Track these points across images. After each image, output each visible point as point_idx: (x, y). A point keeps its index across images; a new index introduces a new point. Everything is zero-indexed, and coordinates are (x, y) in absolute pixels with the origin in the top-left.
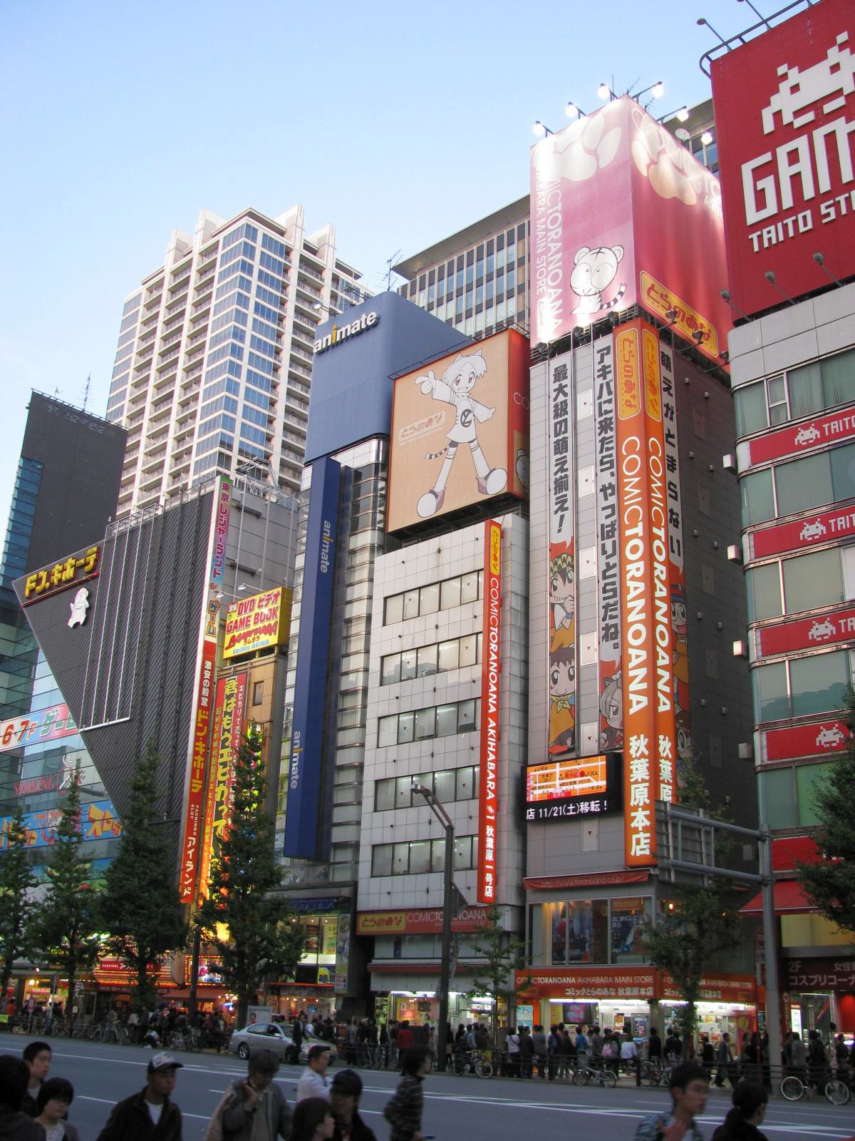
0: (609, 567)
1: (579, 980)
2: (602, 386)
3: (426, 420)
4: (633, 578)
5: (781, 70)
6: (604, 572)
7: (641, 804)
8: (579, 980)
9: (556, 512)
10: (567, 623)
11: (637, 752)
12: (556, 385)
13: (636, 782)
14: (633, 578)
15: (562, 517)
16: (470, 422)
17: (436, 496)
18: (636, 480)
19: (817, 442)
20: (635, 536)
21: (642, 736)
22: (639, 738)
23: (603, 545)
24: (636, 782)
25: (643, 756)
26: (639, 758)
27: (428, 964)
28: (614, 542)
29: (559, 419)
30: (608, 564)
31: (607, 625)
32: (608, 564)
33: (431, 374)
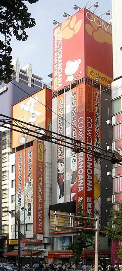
3: (22, 117)
11: (89, 201)
13: (88, 208)
16: (34, 116)
17: (25, 138)
21: (90, 198)
22: (89, 198)
24: (88, 208)
25: (90, 202)
26: (89, 203)
33: (23, 103)
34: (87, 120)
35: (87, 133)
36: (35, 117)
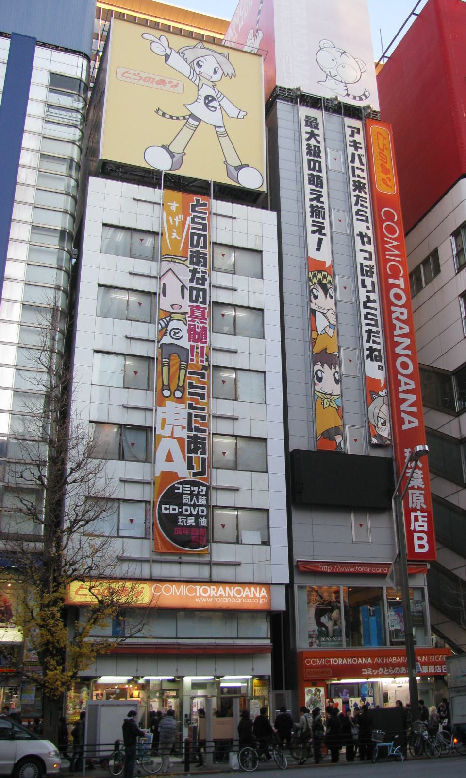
0: (369, 300)
1: (376, 660)
2: (353, 155)
4: (397, 319)
6: (365, 303)
7: (419, 507)
8: (376, 660)
9: (313, 232)
10: (331, 332)
12: (309, 129)
13: (413, 488)
14: (397, 319)
15: (320, 241)
17: (172, 155)
18: (396, 243)
20: (398, 286)
23: (363, 281)
24: (413, 488)
27: (208, 645)
28: (373, 282)
29: (312, 158)
30: (368, 297)
31: (371, 347)
32: (368, 297)
34: (384, 218)
35: (387, 253)
36: (218, 110)
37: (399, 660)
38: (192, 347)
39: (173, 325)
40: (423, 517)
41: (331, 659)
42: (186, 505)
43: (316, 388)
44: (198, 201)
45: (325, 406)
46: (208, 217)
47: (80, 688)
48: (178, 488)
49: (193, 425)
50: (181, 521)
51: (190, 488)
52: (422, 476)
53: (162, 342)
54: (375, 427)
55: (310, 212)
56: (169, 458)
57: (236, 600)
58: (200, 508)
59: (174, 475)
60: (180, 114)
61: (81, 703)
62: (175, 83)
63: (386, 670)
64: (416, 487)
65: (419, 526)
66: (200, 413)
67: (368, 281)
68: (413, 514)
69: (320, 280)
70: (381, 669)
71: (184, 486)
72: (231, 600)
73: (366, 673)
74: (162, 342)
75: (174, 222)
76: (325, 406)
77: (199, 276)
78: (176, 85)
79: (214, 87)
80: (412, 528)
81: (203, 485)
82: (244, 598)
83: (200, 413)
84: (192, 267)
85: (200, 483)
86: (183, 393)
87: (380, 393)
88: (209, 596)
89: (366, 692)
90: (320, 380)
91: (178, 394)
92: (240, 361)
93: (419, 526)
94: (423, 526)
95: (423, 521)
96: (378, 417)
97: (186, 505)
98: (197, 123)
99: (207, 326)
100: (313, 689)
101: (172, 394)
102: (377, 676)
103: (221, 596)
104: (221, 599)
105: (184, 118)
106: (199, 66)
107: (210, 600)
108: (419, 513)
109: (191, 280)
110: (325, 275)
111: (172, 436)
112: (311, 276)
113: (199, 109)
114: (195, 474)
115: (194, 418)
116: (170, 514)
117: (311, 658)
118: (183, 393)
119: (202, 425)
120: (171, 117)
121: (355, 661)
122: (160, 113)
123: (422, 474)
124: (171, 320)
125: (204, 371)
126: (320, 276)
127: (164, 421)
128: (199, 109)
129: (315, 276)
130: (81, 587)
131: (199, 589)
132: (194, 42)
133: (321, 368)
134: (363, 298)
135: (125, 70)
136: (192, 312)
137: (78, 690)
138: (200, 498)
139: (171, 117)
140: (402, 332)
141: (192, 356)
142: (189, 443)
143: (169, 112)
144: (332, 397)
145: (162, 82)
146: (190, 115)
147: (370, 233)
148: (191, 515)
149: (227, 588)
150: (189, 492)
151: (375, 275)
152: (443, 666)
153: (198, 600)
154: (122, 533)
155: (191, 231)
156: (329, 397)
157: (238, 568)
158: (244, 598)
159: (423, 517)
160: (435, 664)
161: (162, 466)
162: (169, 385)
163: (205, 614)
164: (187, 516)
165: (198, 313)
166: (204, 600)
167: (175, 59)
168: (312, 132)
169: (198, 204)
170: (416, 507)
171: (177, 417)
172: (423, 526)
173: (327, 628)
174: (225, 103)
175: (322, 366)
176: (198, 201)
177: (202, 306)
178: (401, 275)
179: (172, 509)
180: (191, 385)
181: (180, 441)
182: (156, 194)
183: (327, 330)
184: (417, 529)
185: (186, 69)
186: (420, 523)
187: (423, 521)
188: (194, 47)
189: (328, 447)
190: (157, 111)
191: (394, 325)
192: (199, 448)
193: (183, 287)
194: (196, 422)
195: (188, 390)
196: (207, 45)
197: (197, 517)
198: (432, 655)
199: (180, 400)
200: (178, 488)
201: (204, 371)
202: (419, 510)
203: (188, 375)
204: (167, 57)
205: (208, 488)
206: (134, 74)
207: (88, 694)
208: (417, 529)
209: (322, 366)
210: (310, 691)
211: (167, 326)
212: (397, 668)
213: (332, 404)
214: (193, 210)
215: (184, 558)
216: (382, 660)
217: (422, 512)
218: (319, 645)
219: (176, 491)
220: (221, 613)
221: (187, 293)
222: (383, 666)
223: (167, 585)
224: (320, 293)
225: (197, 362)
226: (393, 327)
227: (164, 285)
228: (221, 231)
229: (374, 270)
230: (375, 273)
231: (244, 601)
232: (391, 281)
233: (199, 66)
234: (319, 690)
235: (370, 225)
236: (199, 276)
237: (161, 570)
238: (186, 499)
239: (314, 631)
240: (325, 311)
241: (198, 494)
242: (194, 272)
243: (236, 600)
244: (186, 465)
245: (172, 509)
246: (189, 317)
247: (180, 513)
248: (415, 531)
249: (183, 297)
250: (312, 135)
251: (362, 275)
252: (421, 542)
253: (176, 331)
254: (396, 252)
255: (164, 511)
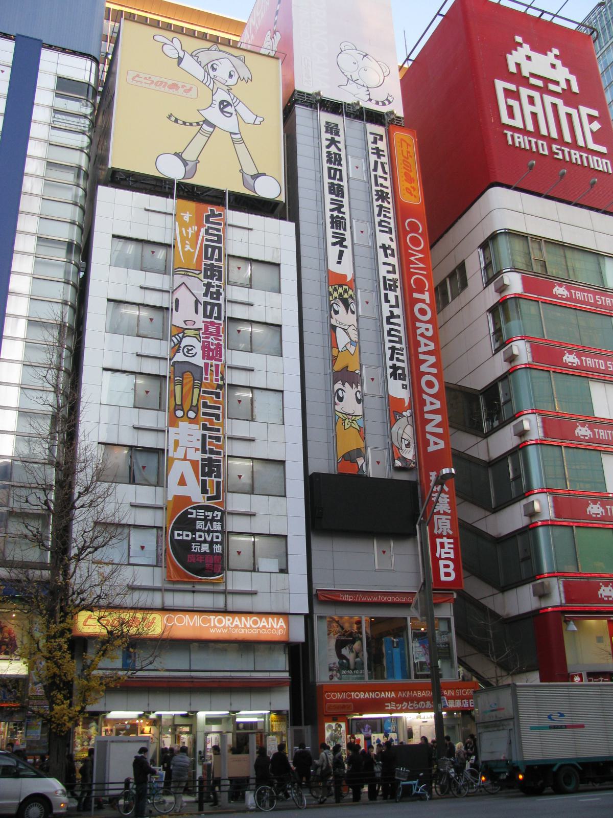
0: (392, 316)
1: (400, 694)
2: (376, 163)
4: (422, 335)
5: (519, 39)
6: (388, 318)
7: (445, 534)
8: (400, 694)
9: (334, 244)
10: (352, 349)
12: (329, 136)
14: (422, 335)
15: (341, 254)
17: (185, 163)
18: (421, 256)
19: (567, 299)
20: (423, 301)
23: (386, 295)
27: (224, 678)
28: (396, 297)
29: (332, 166)
30: (391, 312)
31: (394, 365)
32: (391, 312)
34: (408, 229)
35: (411, 266)
36: (234, 116)
37: (424, 694)
38: (206, 364)
39: (186, 341)
40: (449, 543)
41: (353, 693)
42: (200, 530)
43: (337, 408)
44: (212, 211)
45: (347, 427)
46: (223, 229)
47: (89, 723)
48: (192, 513)
49: (208, 447)
50: (195, 548)
51: (204, 513)
52: (448, 500)
53: (175, 359)
54: (399, 449)
55: (331, 223)
56: (182, 482)
57: (252, 631)
58: (215, 534)
59: (187, 500)
60: (194, 120)
61: (90, 739)
62: (188, 87)
63: (410, 705)
64: (442, 512)
65: (445, 553)
66: (214, 434)
67: (392, 296)
68: (438, 541)
69: (341, 295)
70: (405, 703)
71: (198, 511)
72: (247, 631)
73: (389, 708)
74: (175, 359)
75: (187, 233)
76: (347, 427)
77: (213, 290)
78: (190, 90)
79: (229, 91)
80: (438, 555)
81: (218, 510)
82: (261, 629)
83: (214, 434)
84: (206, 281)
85: (214, 508)
86: (197, 413)
87: (404, 413)
88: (224, 627)
89: (389, 728)
90: (341, 399)
91: (192, 414)
92: (257, 380)
93: (445, 553)
94: (449, 553)
95: (449, 548)
96: (402, 438)
97: (200, 530)
98: (211, 130)
99: (222, 343)
100: (334, 724)
101: (186, 414)
102: (401, 711)
103: (237, 626)
104: (236, 630)
105: (198, 124)
106: (214, 69)
107: (225, 631)
108: (445, 540)
109: (205, 295)
110: (346, 289)
111: (185, 459)
112: (331, 290)
113: (214, 115)
114: (209, 499)
115: (208, 440)
116: (183, 540)
117: (331, 692)
118: (197, 413)
119: (217, 446)
120: (184, 123)
121: (377, 695)
122: (173, 119)
123: (448, 498)
124: (184, 337)
125: (218, 391)
126: (340, 290)
127: (177, 443)
128: (214, 115)
129: (335, 290)
130: (90, 617)
131: (214, 619)
132: (208, 45)
133: (342, 387)
134: (386, 313)
135: (136, 74)
136: (206, 328)
137: (86, 725)
138: (215, 523)
139: (184, 123)
140: (428, 349)
141: (206, 374)
142: (203, 466)
143: (182, 118)
144: (354, 417)
145: (174, 86)
146: (204, 121)
147: (394, 245)
148: (205, 541)
149: (243, 619)
150: (203, 517)
151: (398, 290)
152: (470, 701)
153: (212, 631)
154: (132, 561)
155: (205, 243)
156: (350, 417)
157: (255, 598)
158: (261, 629)
159: (449, 543)
160: (462, 698)
161: (174, 490)
162: (181, 405)
163: (220, 646)
164: (201, 542)
165: (212, 329)
166: (219, 631)
167: (188, 63)
168: (333, 138)
169: (213, 214)
170: (441, 533)
171: (190, 438)
172: (449, 553)
173: (348, 660)
174: (240, 108)
175: (343, 385)
176: (212, 211)
177: (216, 321)
178: (426, 289)
179: (185, 536)
180: (205, 405)
181: (194, 463)
182: (168, 204)
183: (348, 347)
184: (443, 556)
185: (199, 73)
186: (446, 550)
187: (449, 548)
188: (208, 49)
189: (349, 470)
190: (170, 117)
191: (419, 342)
192: (214, 471)
193: (197, 302)
194: (210, 443)
195: (202, 410)
196: (222, 47)
197: (211, 543)
198: (458, 689)
199: (193, 421)
200: (192, 513)
201: (218, 391)
202: (445, 536)
203: (202, 394)
204: (180, 60)
205: (223, 513)
206: (146, 78)
207: (97, 730)
208: (443, 556)
209: (343, 385)
210: (330, 727)
211: (180, 342)
212: (422, 702)
213: (353, 425)
214: (208, 221)
215: (198, 587)
216: (406, 694)
217: (448, 538)
218: (340, 679)
219: (189, 516)
220: (236, 645)
221: (201, 308)
222: (407, 700)
223: (180, 615)
224: (341, 308)
225: (212, 380)
226: (418, 344)
227: (177, 300)
228: (236, 243)
229: (398, 284)
230: (399, 287)
231: (261, 632)
232: (415, 295)
233: (214, 69)
234: (340, 726)
235: (393, 236)
236: (213, 290)
237: (173, 600)
238: (200, 525)
239: (334, 664)
240: (346, 327)
241: (213, 520)
242: (208, 286)
243: (252, 631)
244: (199, 489)
245: (185, 536)
246: (203, 333)
247: (194, 540)
248: (440, 558)
249: (197, 312)
250: (333, 142)
251: (385, 289)
252: (447, 570)
253: (190, 348)
254: (421, 265)
255: (176, 537)
